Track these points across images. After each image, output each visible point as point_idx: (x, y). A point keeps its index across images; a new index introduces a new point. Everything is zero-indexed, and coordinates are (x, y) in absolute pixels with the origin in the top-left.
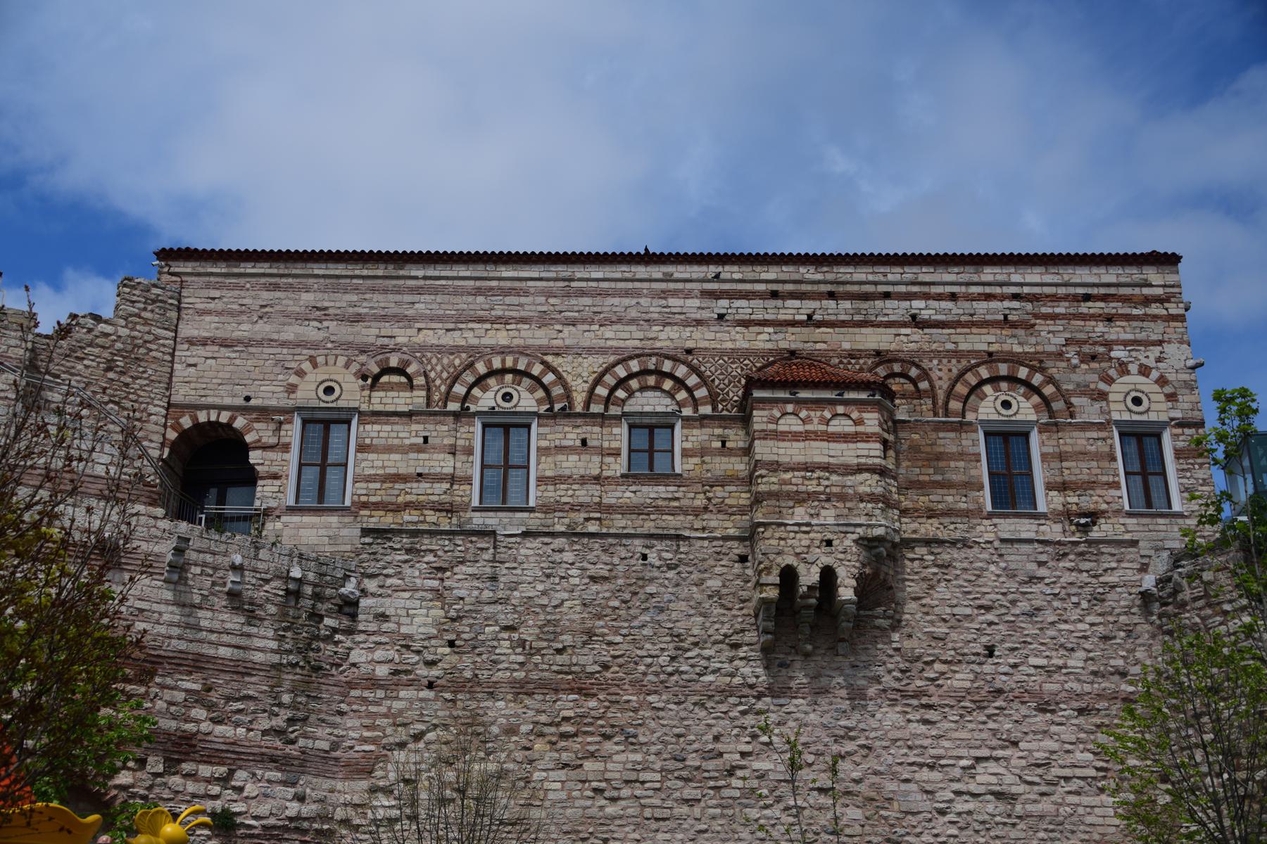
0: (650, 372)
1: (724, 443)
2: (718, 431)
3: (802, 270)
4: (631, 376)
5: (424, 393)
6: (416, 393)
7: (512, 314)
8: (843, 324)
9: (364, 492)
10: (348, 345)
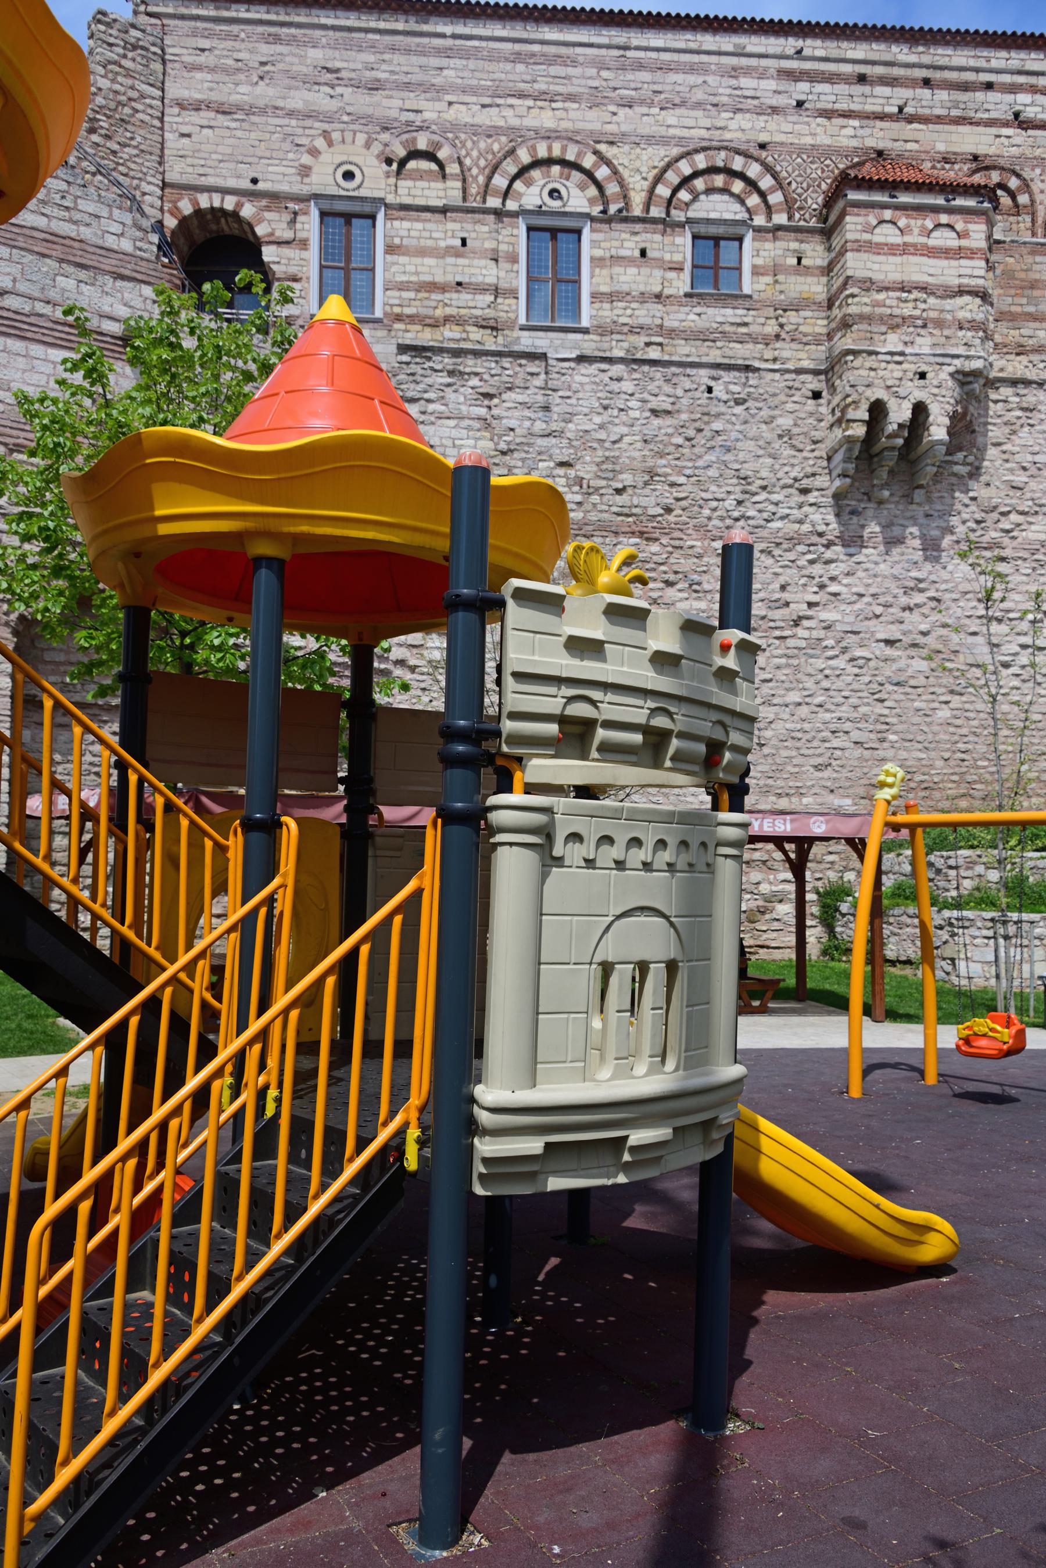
1: (799, 259)
2: (794, 245)
3: (895, 49)
4: (696, 174)
5: (459, 184)
6: (450, 183)
7: (560, 89)
8: (939, 120)
9: (397, 302)
10: (366, 120)
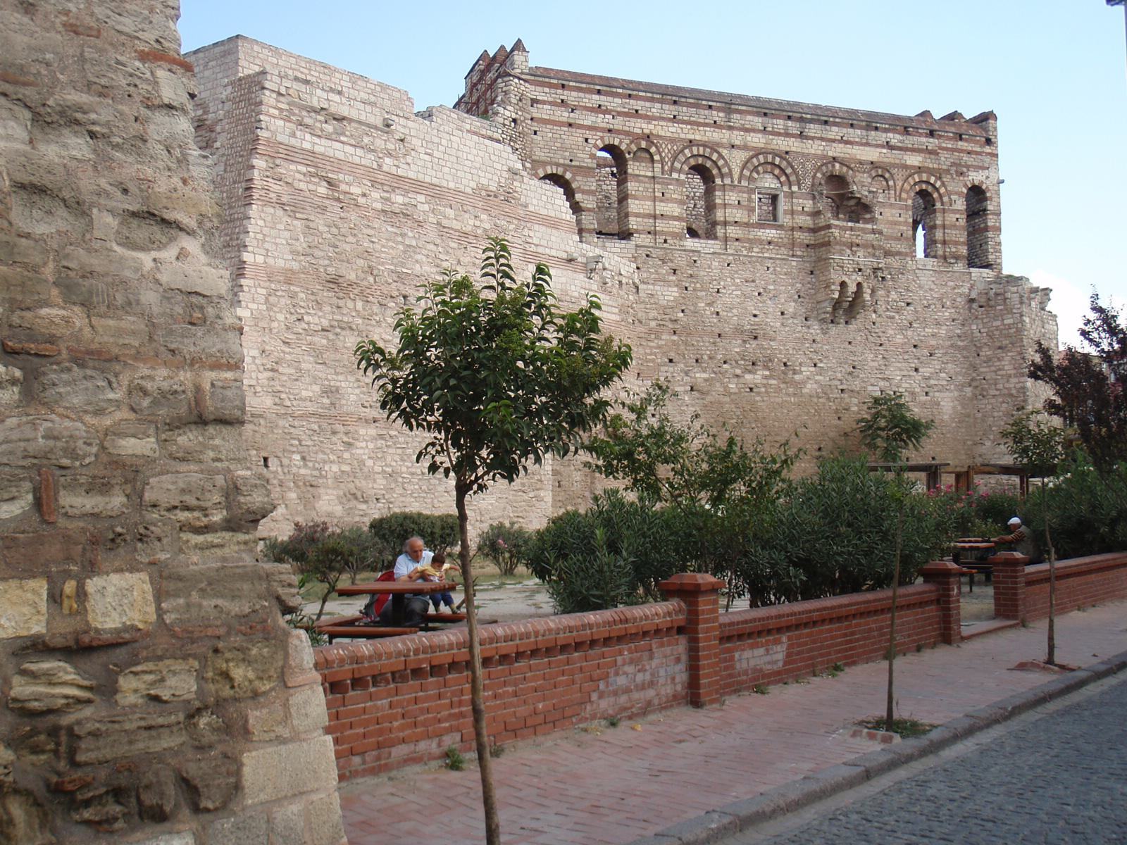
0: (768, 163)
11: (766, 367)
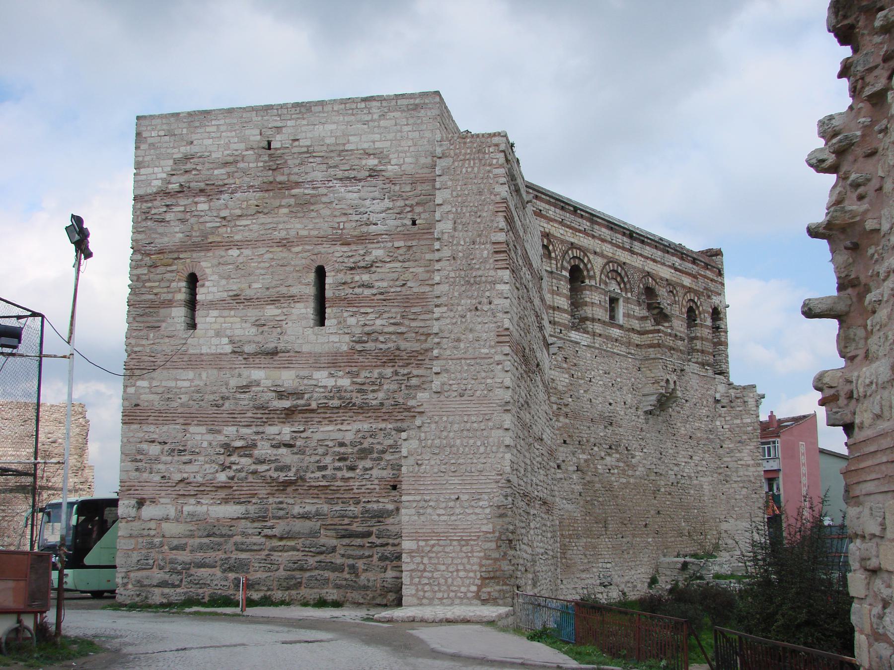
11: (617, 452)
